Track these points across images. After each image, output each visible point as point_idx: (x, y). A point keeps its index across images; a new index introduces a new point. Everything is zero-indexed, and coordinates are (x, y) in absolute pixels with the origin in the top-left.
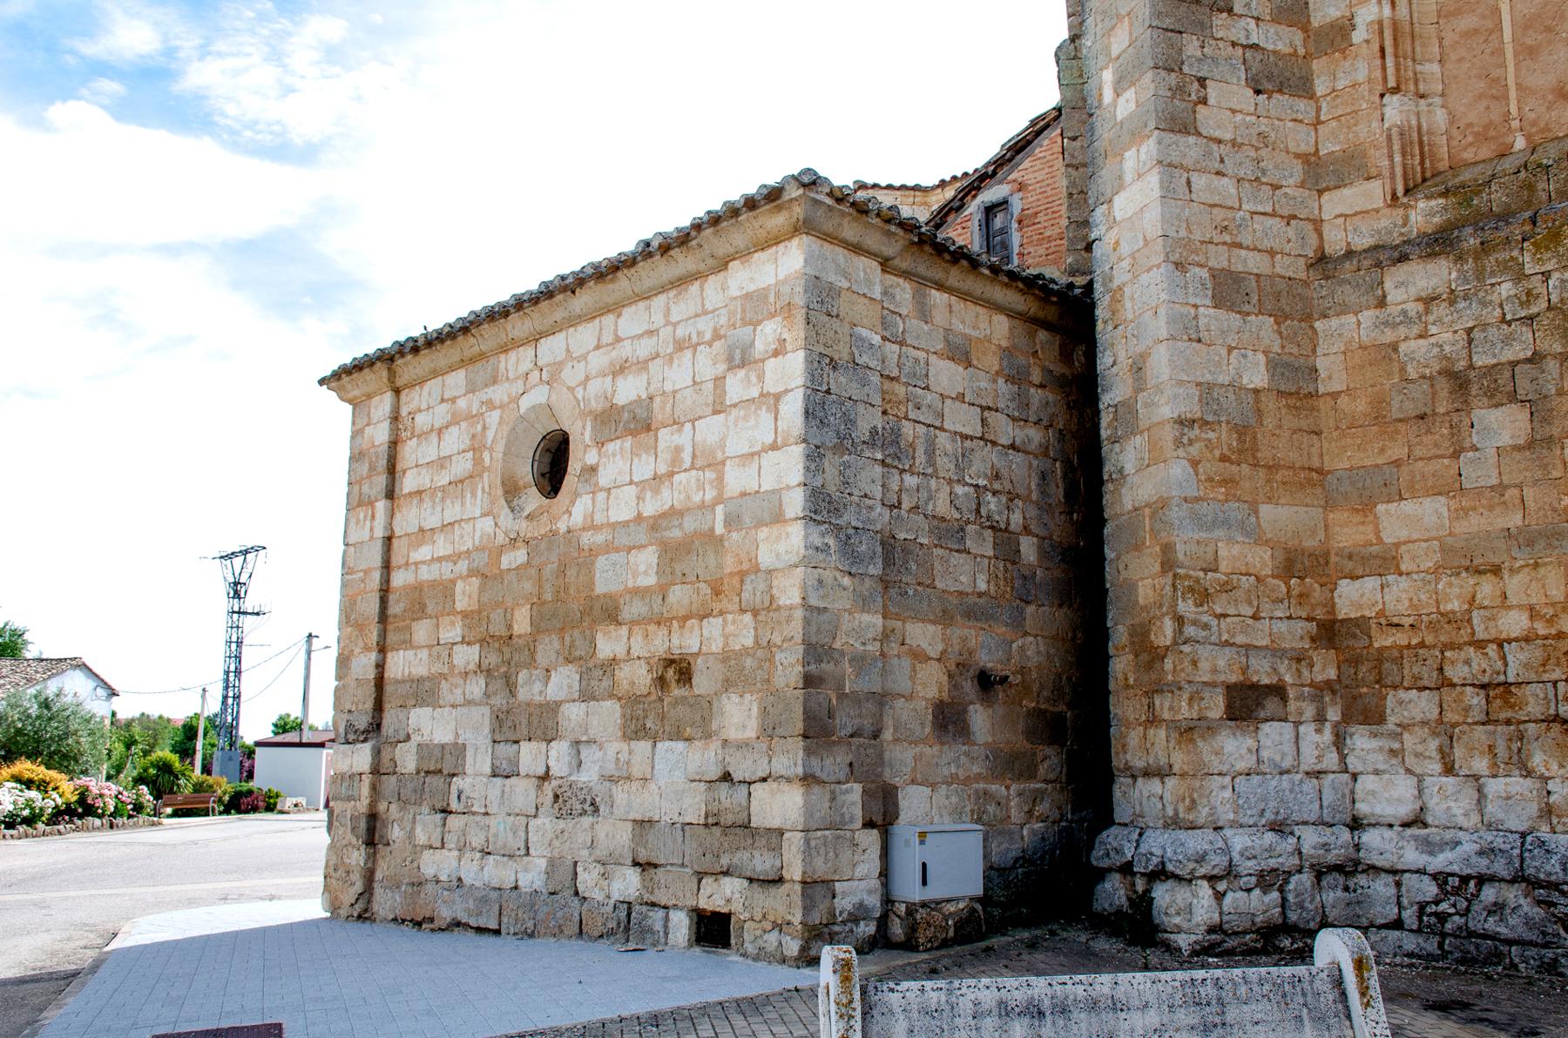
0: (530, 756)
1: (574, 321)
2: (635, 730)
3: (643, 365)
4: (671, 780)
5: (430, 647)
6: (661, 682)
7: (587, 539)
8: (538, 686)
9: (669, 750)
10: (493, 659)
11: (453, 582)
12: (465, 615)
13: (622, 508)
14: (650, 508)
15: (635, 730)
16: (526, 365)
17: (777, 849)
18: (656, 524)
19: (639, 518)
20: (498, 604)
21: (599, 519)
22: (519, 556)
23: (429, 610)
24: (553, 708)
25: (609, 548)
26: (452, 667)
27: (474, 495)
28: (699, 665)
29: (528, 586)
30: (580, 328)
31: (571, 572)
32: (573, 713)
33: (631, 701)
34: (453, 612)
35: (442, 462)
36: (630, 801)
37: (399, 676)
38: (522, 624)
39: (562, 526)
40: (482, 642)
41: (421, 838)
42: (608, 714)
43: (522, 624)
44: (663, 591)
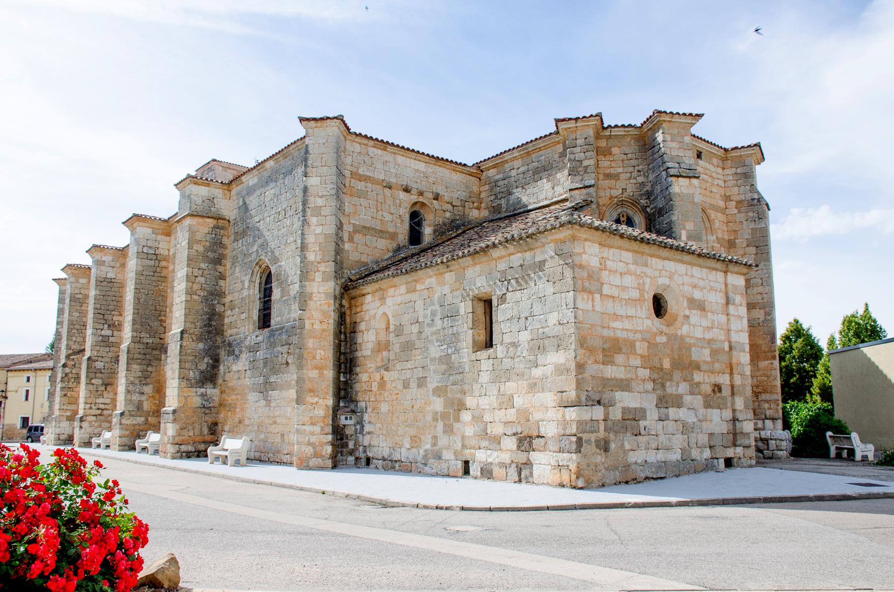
0: (672, 412)
1: (682, 262)
2: (707, 405)
3: (702, 289)
4: (717, 421)
5: (625, 367)
6: (713, 390)
7: (688, 340)
8: (674, 388)
9: (716, 412)
10: (655, 376)
11: (635, 341)
12: (642, 356)
13: (699, 333)
14: (708, 336)
15: (707, 405)
16: (660, 267)
17: (749, 438)
18: (710, 342)
19: (704, 339)
20: (656, 355)
21: (692, 334)
22: (664, 339)
23: (624, 350)
24: (680, 397)
25: (695, 345)
26: (637, 377)
27: (641, 308)
28: (723, 386)
29: (668, 351)
30: (680, 264)
31: (684, 350)
32: (688, 399)
33: (706, 397)
34: (635, 354)
35: (624, 288)
36: (708, 427)
37: (609, 377)
38: (667, 364)
39: (679, 333)
40: (650, 368)
41: (627, 446)
42: (698, 400)
43: (667, 364)
44: (713, 363)
